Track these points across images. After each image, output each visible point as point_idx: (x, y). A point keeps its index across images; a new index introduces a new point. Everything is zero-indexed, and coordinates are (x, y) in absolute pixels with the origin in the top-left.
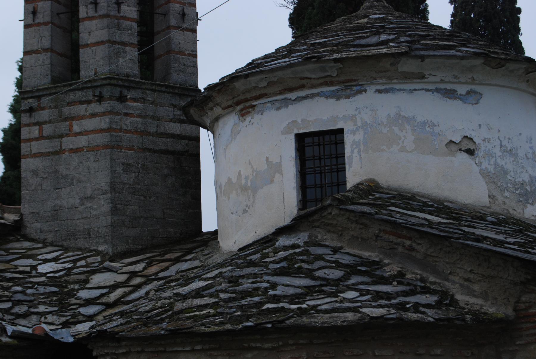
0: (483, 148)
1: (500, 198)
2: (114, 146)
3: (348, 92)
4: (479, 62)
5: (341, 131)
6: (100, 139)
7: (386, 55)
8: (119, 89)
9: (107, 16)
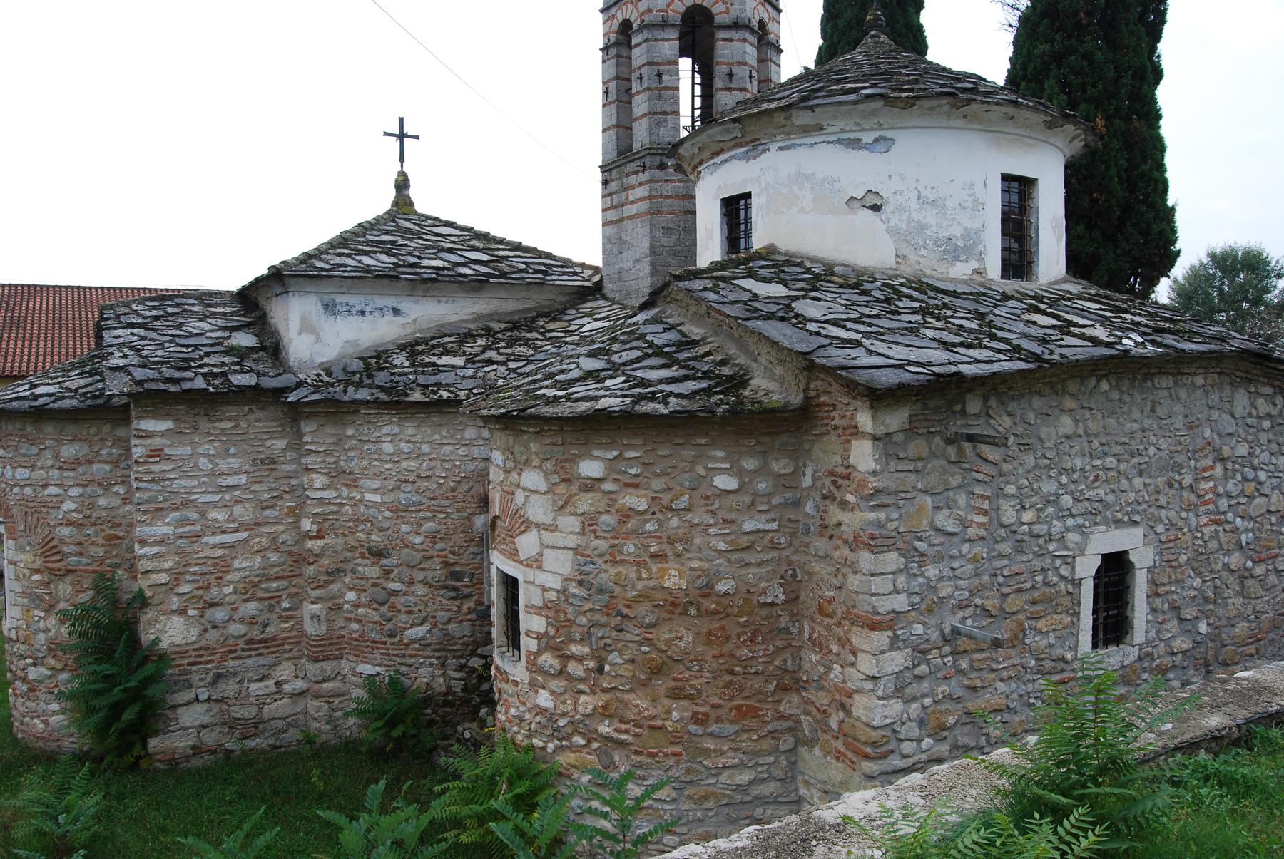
0: (892, 202)
1: (913, 258)
2: (654, 212)
3: (755, 152)
4: (879, 104)
5: (748, 196)
6: (644, 206)
7: (776, 109)
8: (659, 158)
9: (649, 89)
